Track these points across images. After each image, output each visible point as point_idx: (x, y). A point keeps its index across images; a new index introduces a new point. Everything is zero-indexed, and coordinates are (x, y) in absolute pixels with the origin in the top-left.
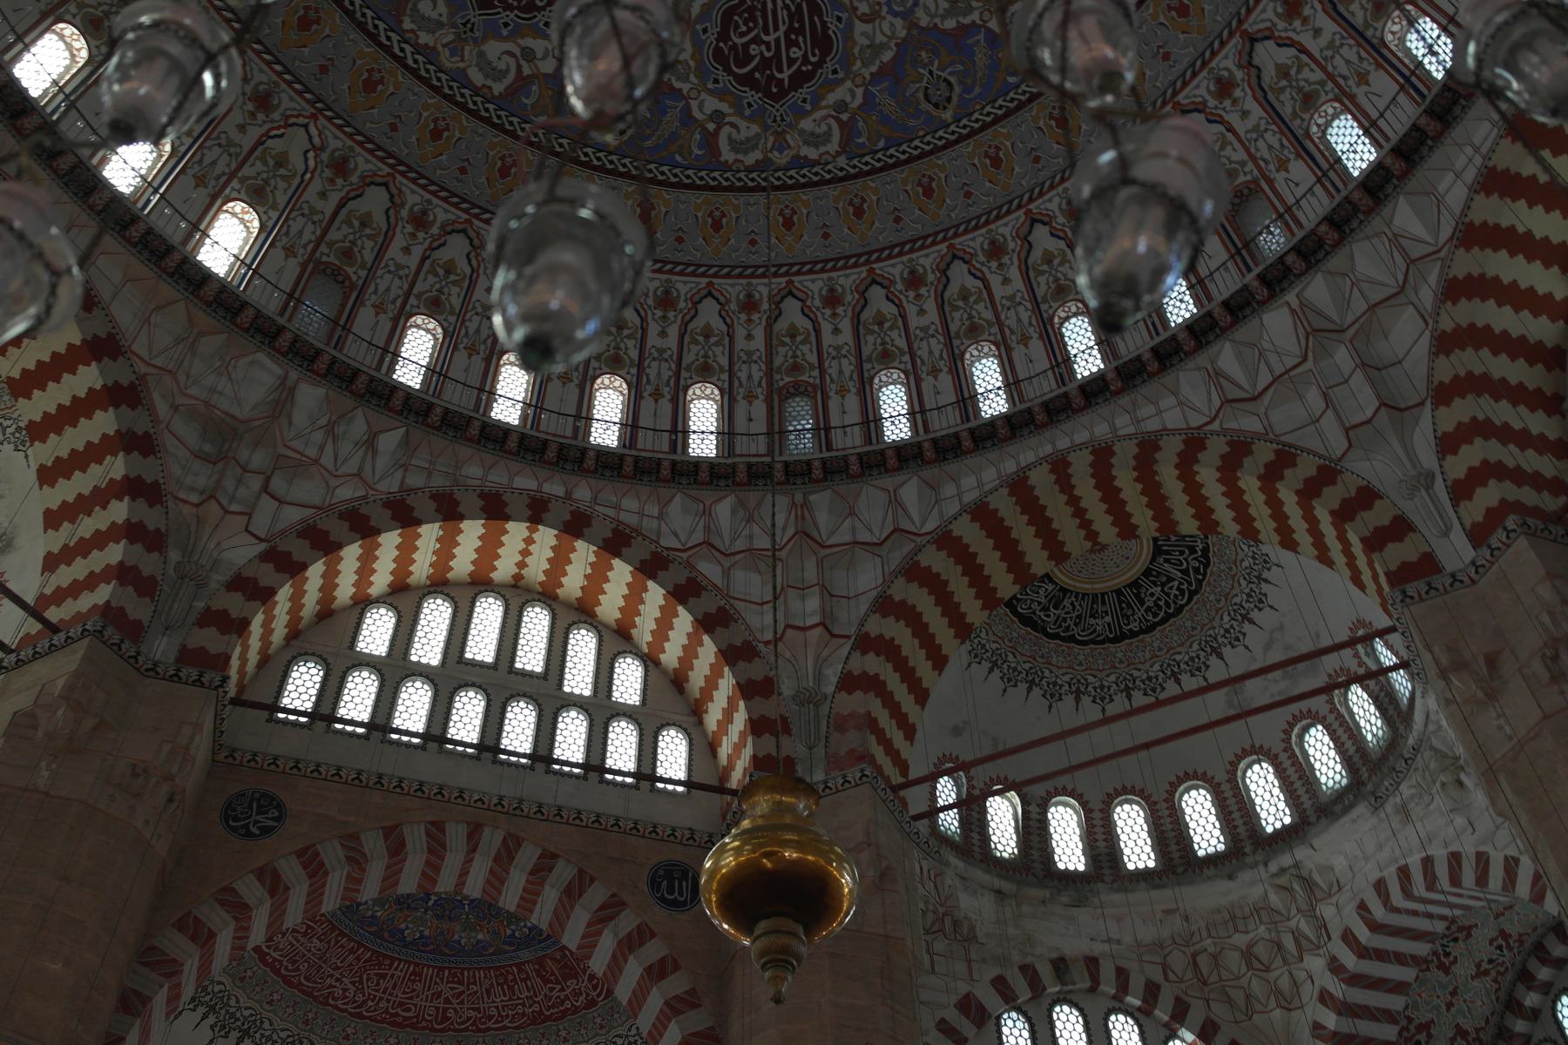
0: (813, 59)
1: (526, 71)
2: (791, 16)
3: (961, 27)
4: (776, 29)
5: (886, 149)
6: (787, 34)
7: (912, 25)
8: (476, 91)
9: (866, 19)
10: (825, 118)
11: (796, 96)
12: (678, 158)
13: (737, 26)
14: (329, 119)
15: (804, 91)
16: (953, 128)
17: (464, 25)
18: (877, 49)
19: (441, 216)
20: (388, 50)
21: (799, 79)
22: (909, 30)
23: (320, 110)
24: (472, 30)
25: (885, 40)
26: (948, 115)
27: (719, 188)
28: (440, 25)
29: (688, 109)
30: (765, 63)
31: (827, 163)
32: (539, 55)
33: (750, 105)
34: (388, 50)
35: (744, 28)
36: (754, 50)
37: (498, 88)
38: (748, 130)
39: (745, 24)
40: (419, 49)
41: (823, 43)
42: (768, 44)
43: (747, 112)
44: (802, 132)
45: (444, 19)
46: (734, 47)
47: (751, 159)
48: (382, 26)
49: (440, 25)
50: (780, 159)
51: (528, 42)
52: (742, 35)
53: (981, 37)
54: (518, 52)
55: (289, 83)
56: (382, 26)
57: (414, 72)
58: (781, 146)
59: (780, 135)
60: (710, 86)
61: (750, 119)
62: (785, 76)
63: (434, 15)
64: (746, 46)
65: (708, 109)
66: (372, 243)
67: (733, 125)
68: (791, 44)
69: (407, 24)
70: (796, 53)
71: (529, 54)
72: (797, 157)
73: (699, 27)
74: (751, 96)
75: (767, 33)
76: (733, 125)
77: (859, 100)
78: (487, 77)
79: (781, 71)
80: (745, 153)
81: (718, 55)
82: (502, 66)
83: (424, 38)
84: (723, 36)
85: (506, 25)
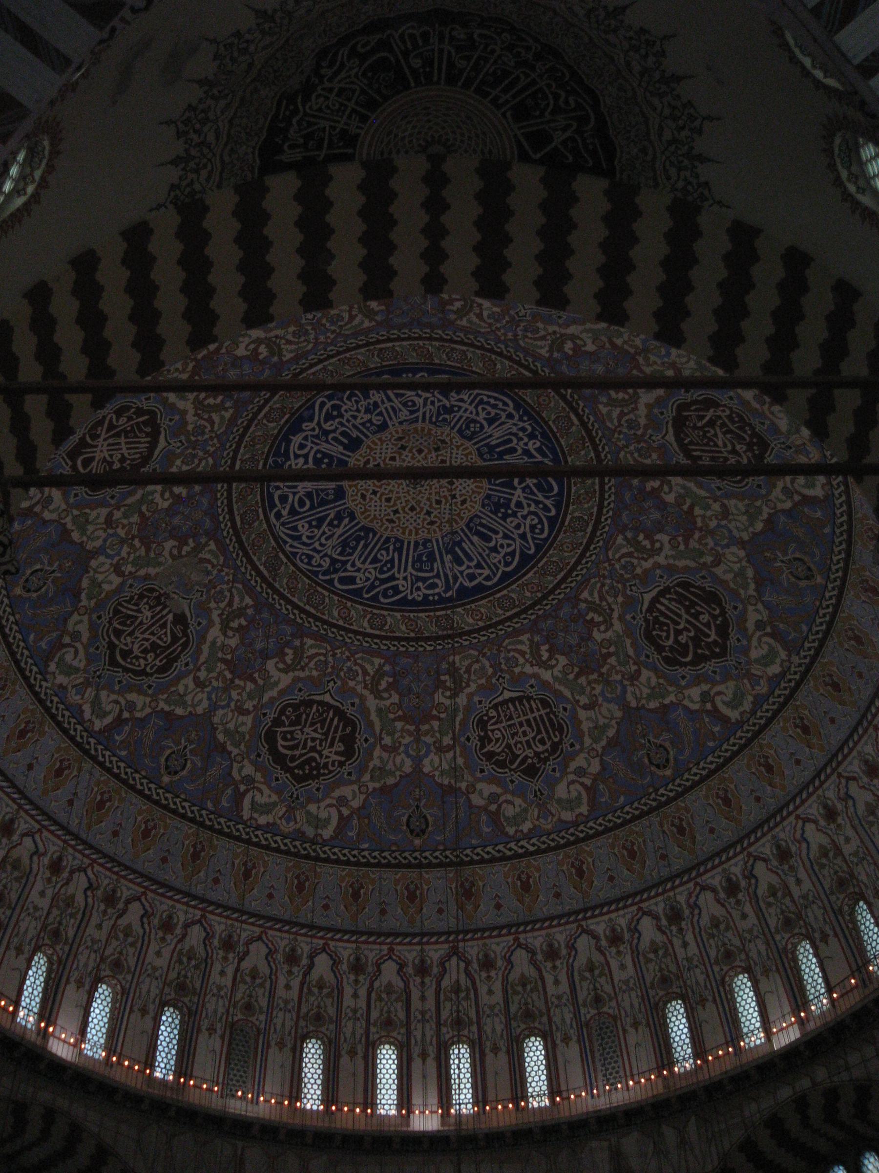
0: (717, 612)
1: (588, 782)
2: (680, 603)
3: (770, 522)
4: (680, 616)
5: (810, 630)
6: (688, 612)
7: (742, 544)
8: (576, 824)
9: (717, 562)
10: (759, 639)
11: (732, 642)
12: (711, 744)
13: (660, 637)
14: (525, 932)
15: (733, 634)
16: (830, 586)
17: (536, 796)
18: (741, 573)
19: (623, 922)
20: (517, 856)
21: (723, 631)
22: (744, 548)
23: (517, 932)
24: (542, 794)
25: (738, 565)
26: (819, 580)
27: (750, 741)
28: (525, 811)
29: (686, 708)
30: (696, 640)
31: (789, 668)
32: (585, 766)
33: (715, 672)
34: (517, 856)
35: (664, 634)
36: (683, 639)
37: (584, 809)
38: (728, 689)
39: (662, 631)
40: (528, 837)
41: (712, 598)
42: (686, 629)
43: (718, 678)
44: (757, 661)
45: (524, 805)
46: (671, 647)
47: (747, 706)
48: (500, 847)
49: (525, 811)
50: (762, 688)
51: (573, 766)
52: (668, 638)
53: (783, 518)
54: (572, 777)
55: (490, 937)
56: (500, 847)
57: (539, 852)
58: (754, 680)
59: (749, 675)
60: (683, 683)
61: (723, 682)
62: (713, 637)
63: (518, 810)
64: (676, 641)
65: (697, 698)
66: (604, 978)
67: (719, 693)
68: (696, 616)
69: (511, 831)
70: (705, 618)
71: (581, 772)
72: (770, 679)
73: (643, 658)
74: (709, 667)
75: (679, 624)
76: (719, 693)
77: (765, 613)
78: (572, 810)
79: (708, 636)
80: (741, 704)
81: (668, 661)
82: (574, 794)
83: (526, 827)
84: (660, 649)
85: (554, 770)
